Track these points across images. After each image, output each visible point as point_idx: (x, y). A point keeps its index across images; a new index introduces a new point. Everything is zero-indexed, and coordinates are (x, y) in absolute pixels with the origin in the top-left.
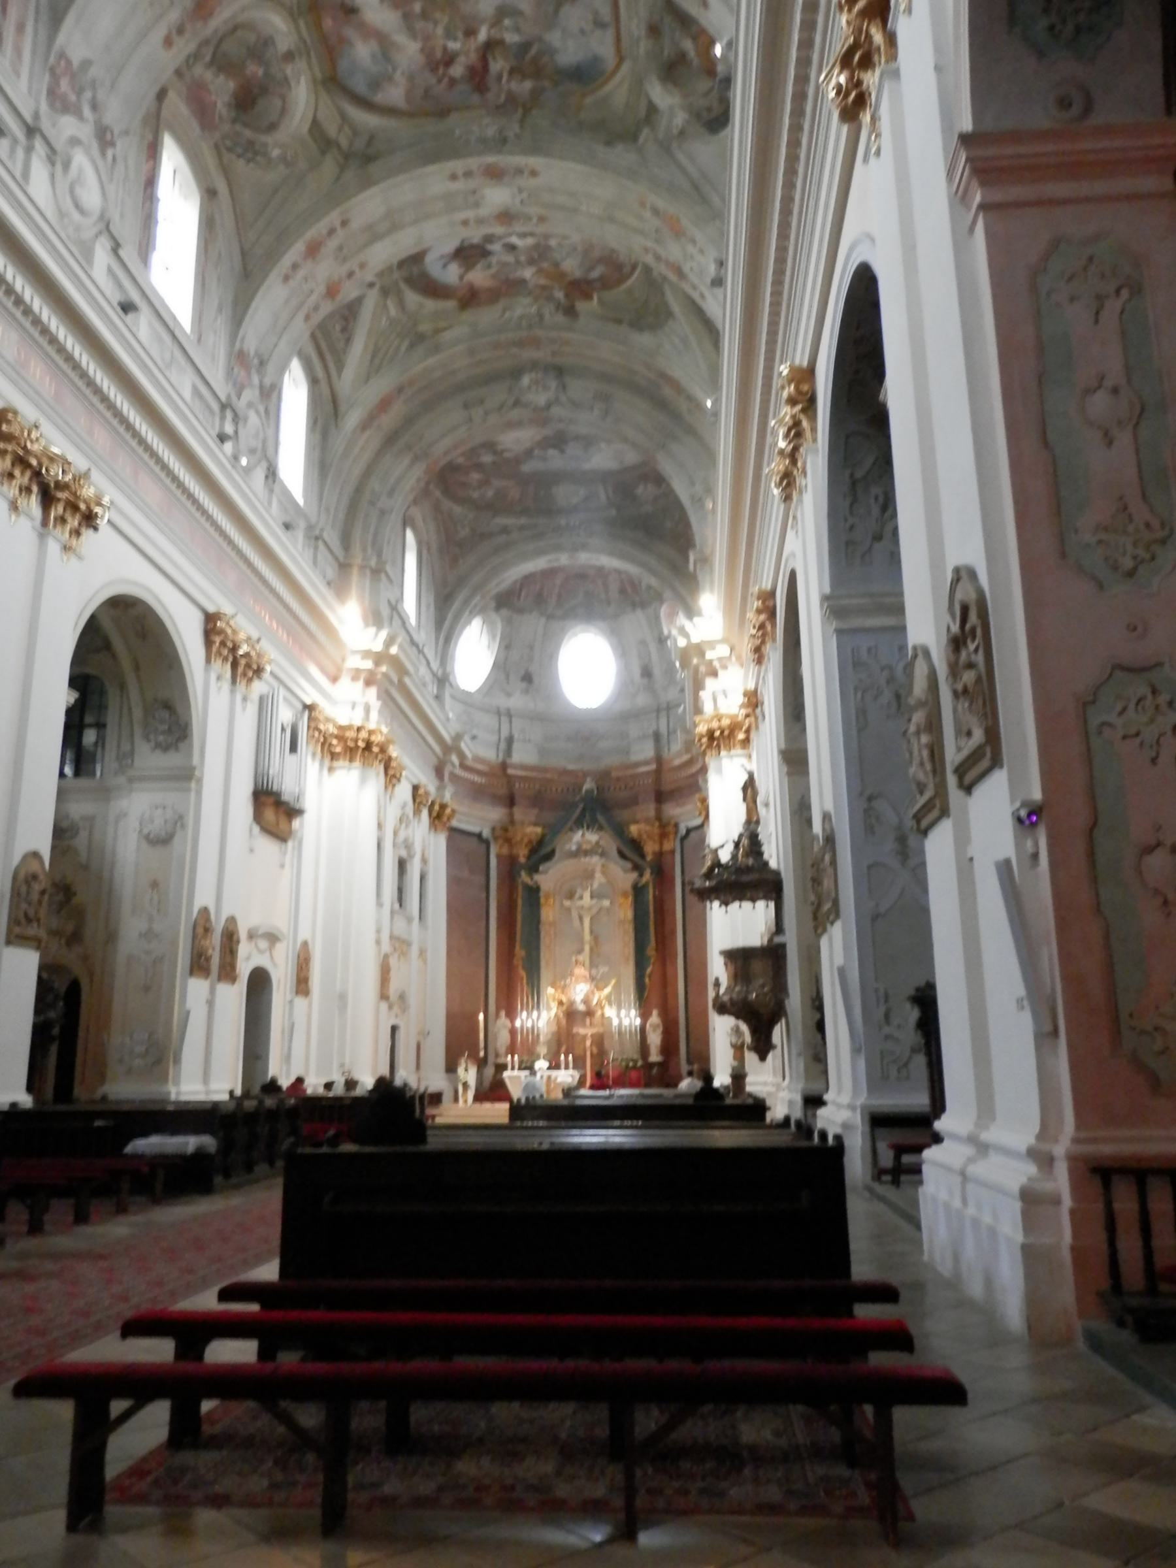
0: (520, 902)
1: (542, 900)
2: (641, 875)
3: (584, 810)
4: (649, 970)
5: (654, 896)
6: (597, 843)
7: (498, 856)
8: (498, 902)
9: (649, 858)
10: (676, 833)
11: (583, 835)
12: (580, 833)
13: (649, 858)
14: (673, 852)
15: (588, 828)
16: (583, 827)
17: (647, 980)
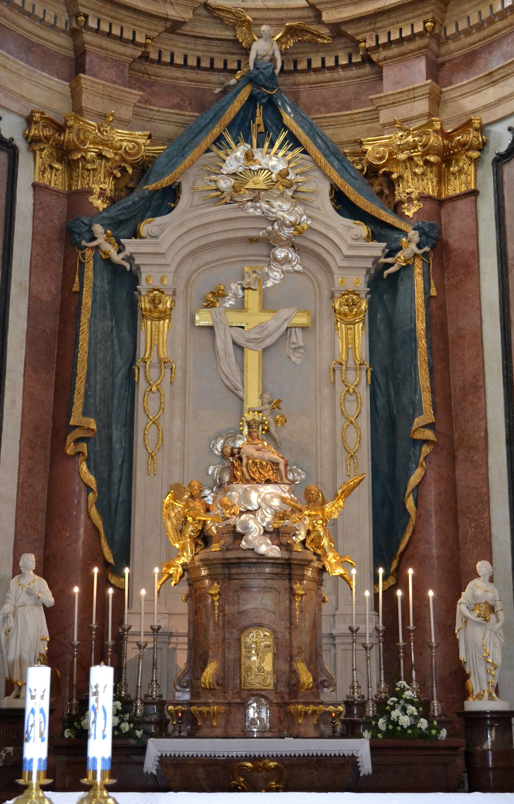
0: (87, 300)
1: (145, 304)
2: (392, 252)
3: (252, 100)
4: (414, 479)
5: (428, 299)
6: (283, 174)
7: (35, 186)
8: (33, 299)
9: (410, 211)
10: (482, 147)
11: (249, 157)
12: (240, 152)
13: (410, 211)
14: (474, 193)
15: (260, 145)
16: (248, 140)
17: (410, 503)
